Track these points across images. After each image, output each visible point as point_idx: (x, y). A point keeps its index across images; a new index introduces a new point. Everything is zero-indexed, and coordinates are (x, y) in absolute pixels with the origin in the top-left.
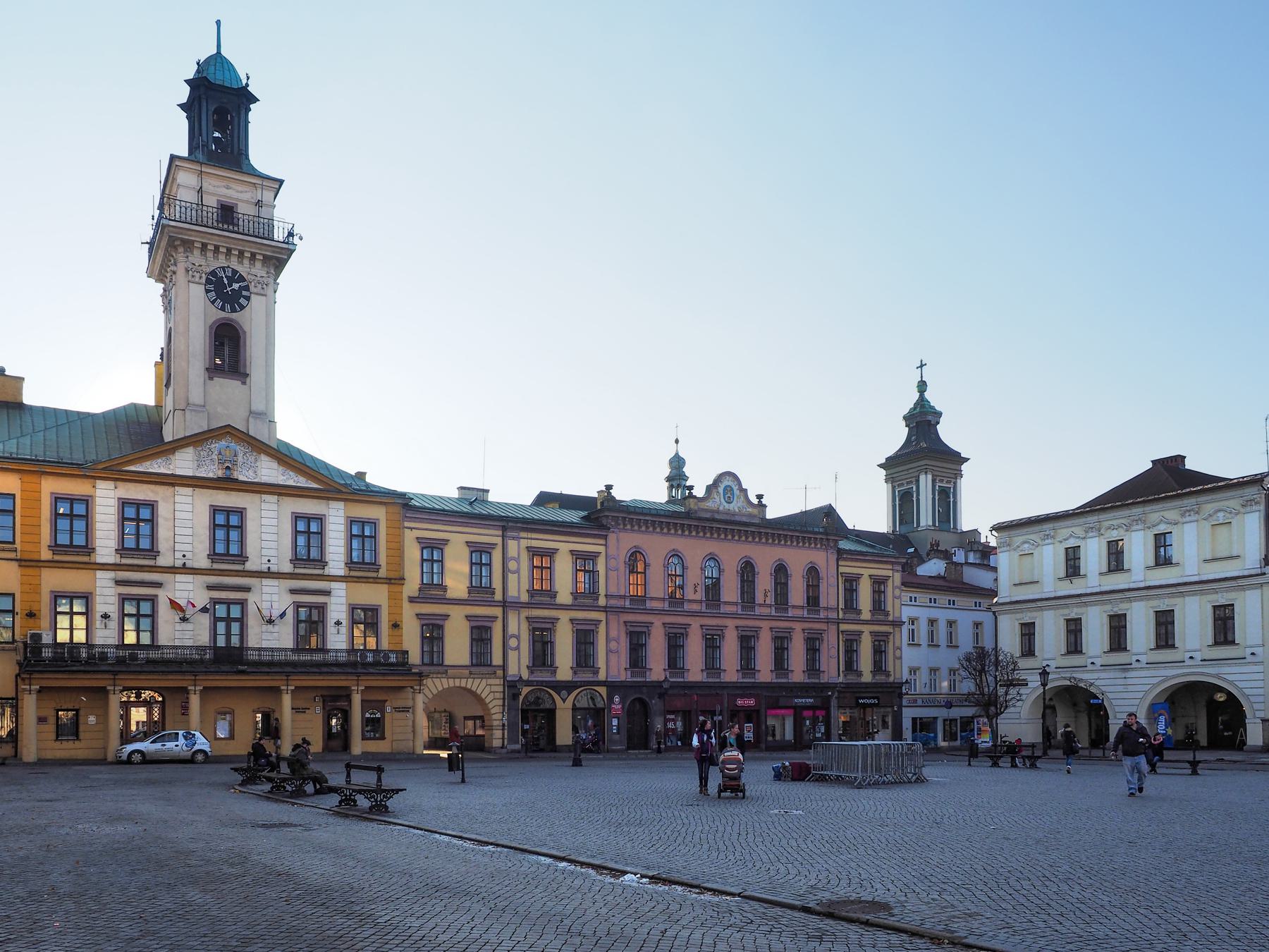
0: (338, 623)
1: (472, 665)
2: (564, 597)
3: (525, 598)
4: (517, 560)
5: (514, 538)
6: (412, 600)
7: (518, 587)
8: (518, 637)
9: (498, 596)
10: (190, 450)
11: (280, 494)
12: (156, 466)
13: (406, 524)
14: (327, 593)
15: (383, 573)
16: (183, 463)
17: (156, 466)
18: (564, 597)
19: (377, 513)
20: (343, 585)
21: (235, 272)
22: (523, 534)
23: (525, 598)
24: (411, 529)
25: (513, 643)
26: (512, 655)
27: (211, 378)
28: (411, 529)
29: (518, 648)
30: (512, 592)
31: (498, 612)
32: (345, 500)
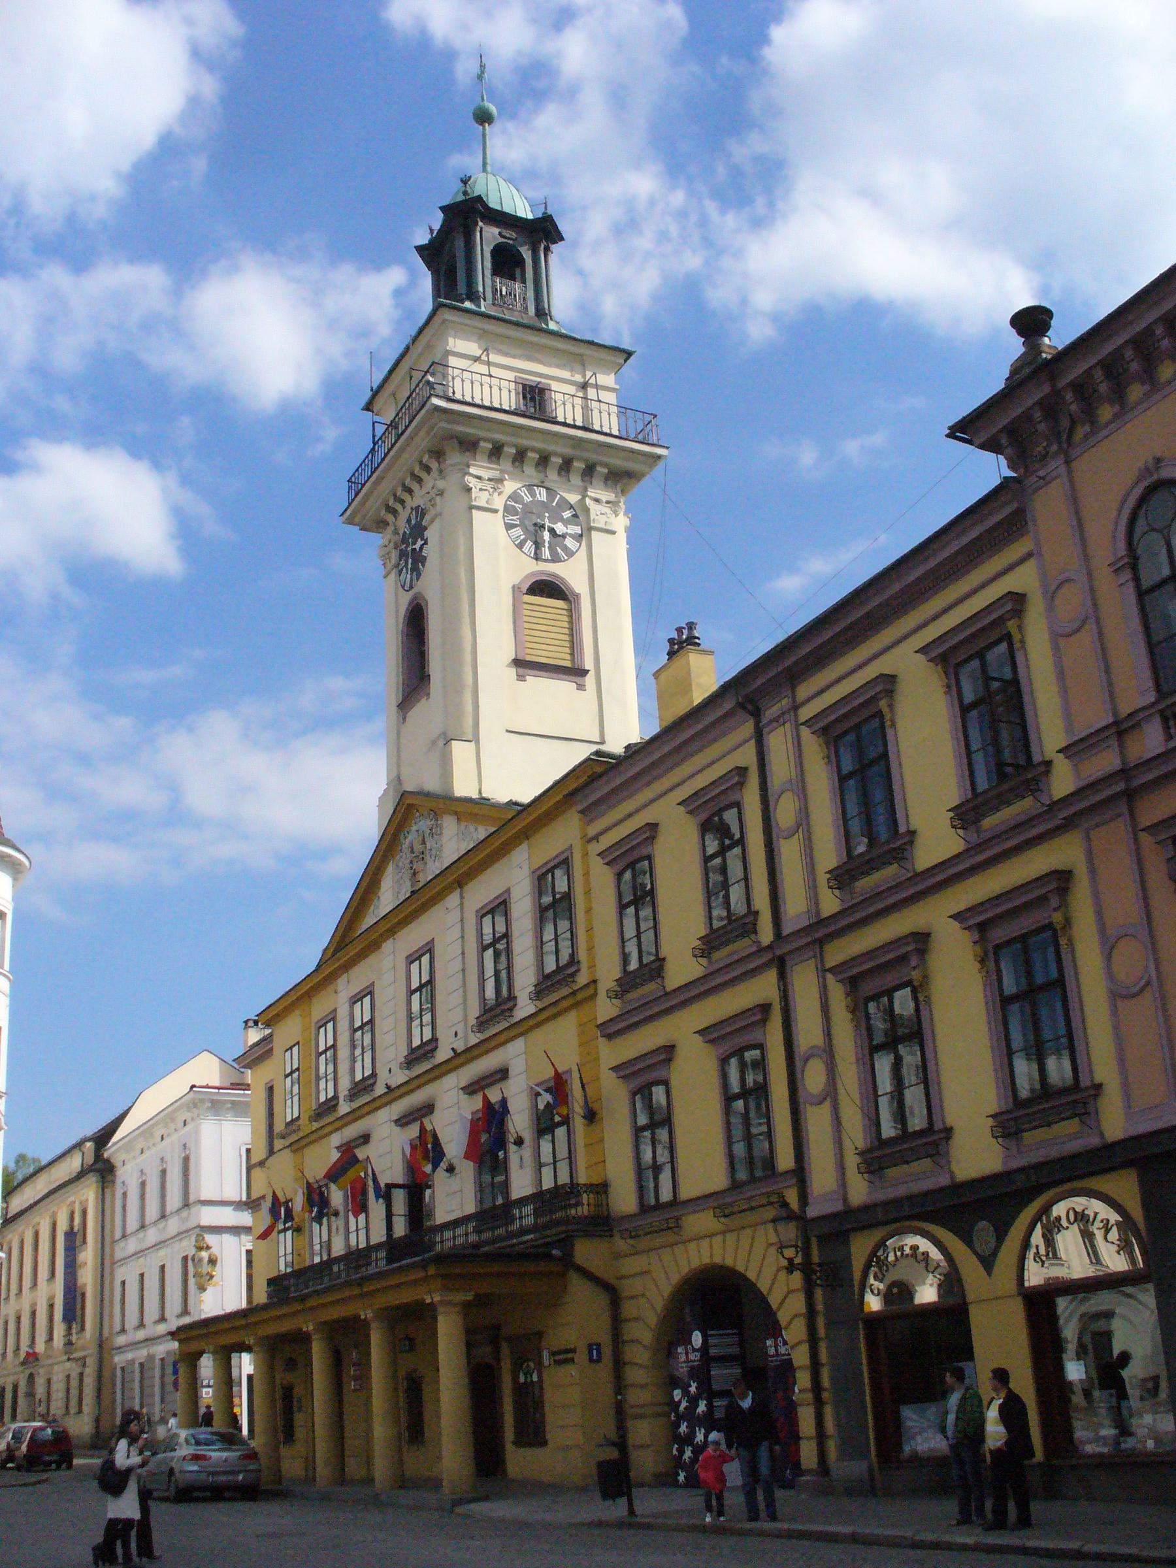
0: (519, 1142)
1: (736, 1185)
2: (936, 840)
3: (830, 903)
4: (800, 788)
5: (777, 720)
6: (611, 1031)
7: (804, 884)
8: (828, 1052)
9: (766, 935)
10: (390, 868)
11: (460, 883)
12: (369, 920)
13: (592, 830)
14: (502, 1074)
15: (582, 979)
16: (387, 898)
17: (369, 920)
18: (936, 840)
19: (565, 834)
20: (518, 1045)
21: (417, 508)
22: (803, 691)
23: (830, 903)
24: (596, 838)
25: (814, 1078)
26: (817, 1120)
27: (404, 719)
28: (596, 838)
29: (831, 1093)
30: (795, 906)
31: (764, 988)
32: (525, 834)
